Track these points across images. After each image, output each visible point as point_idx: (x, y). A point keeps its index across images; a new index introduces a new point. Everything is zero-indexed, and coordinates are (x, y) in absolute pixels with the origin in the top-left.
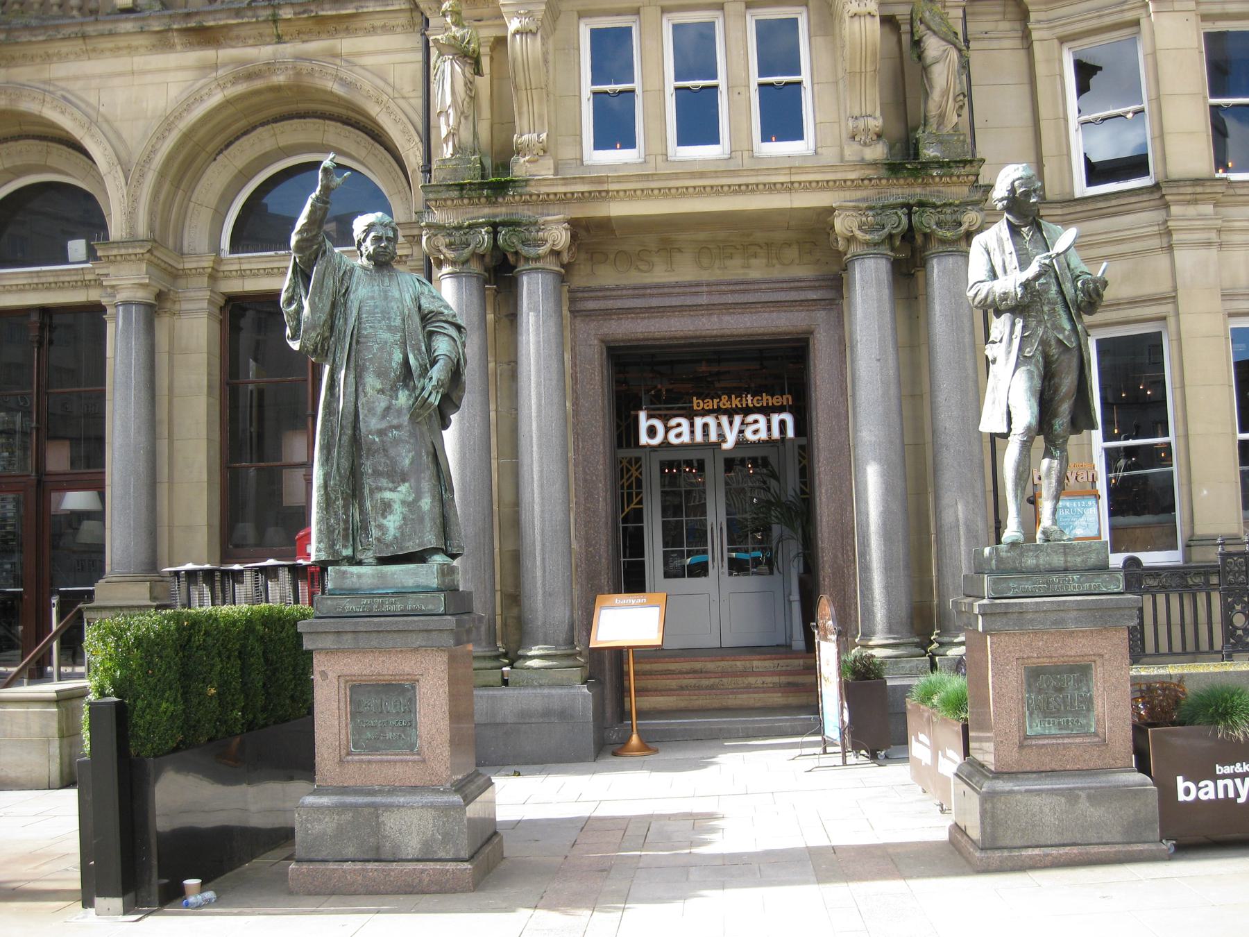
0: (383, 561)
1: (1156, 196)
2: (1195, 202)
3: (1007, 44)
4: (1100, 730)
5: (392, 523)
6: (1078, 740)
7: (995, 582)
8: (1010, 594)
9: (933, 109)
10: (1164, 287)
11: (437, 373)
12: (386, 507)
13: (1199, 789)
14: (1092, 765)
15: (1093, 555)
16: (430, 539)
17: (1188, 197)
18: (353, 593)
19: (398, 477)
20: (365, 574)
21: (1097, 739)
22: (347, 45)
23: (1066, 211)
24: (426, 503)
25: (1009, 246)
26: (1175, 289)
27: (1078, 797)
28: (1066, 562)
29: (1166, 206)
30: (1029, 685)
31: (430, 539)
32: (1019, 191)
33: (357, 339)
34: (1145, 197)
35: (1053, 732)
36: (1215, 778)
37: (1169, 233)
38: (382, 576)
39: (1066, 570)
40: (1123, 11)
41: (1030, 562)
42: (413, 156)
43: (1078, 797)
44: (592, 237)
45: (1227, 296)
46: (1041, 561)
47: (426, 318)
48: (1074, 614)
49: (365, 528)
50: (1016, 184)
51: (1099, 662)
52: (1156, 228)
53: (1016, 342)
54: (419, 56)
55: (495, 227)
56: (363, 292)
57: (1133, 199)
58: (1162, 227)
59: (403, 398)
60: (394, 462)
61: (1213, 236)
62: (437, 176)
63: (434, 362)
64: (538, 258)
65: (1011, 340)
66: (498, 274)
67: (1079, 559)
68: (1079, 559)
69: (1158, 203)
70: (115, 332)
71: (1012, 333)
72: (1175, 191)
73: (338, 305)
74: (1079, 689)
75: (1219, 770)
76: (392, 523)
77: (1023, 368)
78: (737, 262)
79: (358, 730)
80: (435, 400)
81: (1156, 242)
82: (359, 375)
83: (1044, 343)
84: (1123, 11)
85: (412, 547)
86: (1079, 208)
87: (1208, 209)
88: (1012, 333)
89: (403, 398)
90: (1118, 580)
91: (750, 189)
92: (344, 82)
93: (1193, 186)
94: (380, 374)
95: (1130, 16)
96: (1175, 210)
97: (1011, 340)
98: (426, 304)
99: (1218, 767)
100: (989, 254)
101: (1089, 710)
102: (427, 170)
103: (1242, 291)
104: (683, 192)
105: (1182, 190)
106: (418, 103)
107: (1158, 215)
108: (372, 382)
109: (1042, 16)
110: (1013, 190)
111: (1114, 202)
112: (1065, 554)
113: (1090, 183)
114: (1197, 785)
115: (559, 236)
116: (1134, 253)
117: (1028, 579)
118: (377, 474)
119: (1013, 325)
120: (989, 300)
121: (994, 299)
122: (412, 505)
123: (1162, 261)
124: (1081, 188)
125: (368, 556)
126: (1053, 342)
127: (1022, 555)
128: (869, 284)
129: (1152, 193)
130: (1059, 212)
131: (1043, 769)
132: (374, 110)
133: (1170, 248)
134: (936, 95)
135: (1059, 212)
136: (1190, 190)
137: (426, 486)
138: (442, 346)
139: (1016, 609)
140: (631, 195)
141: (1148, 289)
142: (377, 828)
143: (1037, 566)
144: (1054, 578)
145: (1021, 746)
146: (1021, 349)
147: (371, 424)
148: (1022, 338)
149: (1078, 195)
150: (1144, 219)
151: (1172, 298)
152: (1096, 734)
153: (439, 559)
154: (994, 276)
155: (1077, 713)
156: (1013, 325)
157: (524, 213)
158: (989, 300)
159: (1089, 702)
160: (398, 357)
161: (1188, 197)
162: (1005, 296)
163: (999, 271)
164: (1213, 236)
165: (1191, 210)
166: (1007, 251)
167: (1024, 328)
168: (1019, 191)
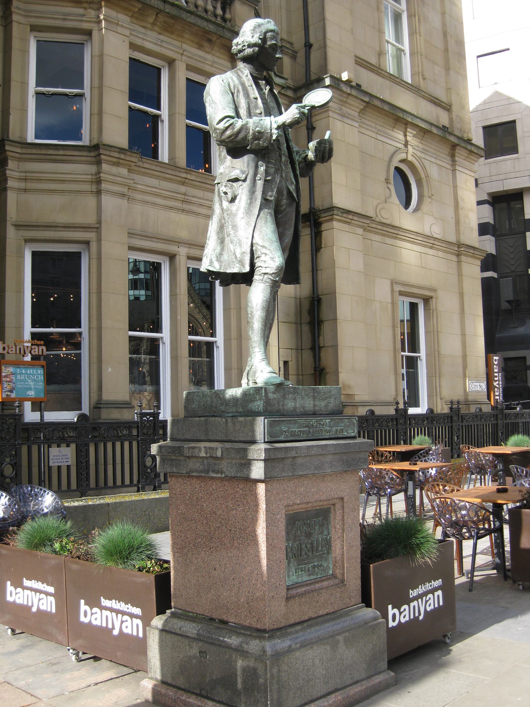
1: (93, 154)
2: (117, 164)
4: (338, 572)
6: (325, 584)
7: (271, 425)
8: (282, 438)
10: (91, 220)
13: (400, 613)
14: (336, 608)
15: (332, 400)
17: (115, 160)
21: (337, 581)
23: (24, 151)
25: (254, 93)
26: (99, 222)
27: (338, 641)
28: (315, 406)
29: (99, 163)
30: (288, 533)
32: (269, 43)
34: (85, 153)
35: (305, 578)
36: (408, 601)
37: (99, 182)
39: (314, 414)
40: (82, 21)
41: (290, 405)
43: (338, 641)
45: (131, 234)
46: (298, 405)
48: (329, 458)
50: (269, 35)
51: (338, 506)
52: (90, 177)
53: (260, 184)
57: (76, 153)
58: (94, 177)
65: (254, 181)
67: (323, 404)
68: (323, 404)
69: (93, 159)
71: (255, 175)
72: (107, 153)
74: (322, 533)
75: (413, 593)
77: (266, 210)
81: (87, 187)
83: (279, 192)
84: (82, 21)
86: (34, 151)
87: (124, 171)
88: (255, 175)
90: (354, 425)
93: (119, 153)
95: (86, 26)
96: (105, 167)
97: (254, 181)
99: (411, 592)
100: (233, 94)
101: (328, 553)
103: (139, 233)
105: (112, 154)
107: (93, 169)
110: (264, 40)
111: (61, 152)
112: (314, 398)
113: (37, 137)
114: (399, 610)
116: (71, 192)
117: (295, 422)
119: (257, 167)
120: (241, 136)
121: (245, 138)
123: (91, 201)
124: (31, 138)
126: (285, 192)
127: (284, 397)
129: (90, 151)
130: (19, 150)
131: (303, 618)
133: (99, 192)
135: (19, 150)
136: (117, 155)
139: (293, 454)
141: (79, 220)
143: (295, 408)
144: (313, 421)
145: (288, 599)
146: (264, 193)
148: (266, 181)
149: (29, 141)
150: (82, 170)
151: (97, 228)
152: (334, 576)
154: (238, 116)
155: (321, 557)
156: (257, 167)
158: (241, 136)
159: (328, 544)
161: (115, 160)
162: (259, 135)
163: (243, 112)
165: (114, 170)
166: (252, 96)
167: (267, 172)
168: (269, 43)
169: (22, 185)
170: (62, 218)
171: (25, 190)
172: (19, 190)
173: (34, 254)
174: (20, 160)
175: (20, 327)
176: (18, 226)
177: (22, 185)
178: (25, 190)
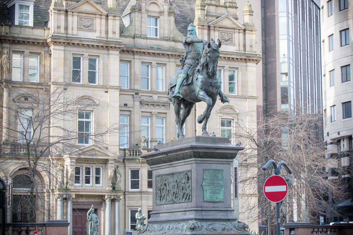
3: (122, 168)
9: (117, 183)
37: (142, 198)
44: (78, 196)
61: (147, 199)
78: (90, 199)
81: (140, 199)
87: (146, 195)
91: (96, 192)
104: (88, 192)
107: (141, 195)
109: (127, 165)
115: (74, 197)
123: (140, 201)
128: (108, 203)
133: (142, 200)
134: (118, 181)
140: (82, 192)
157: (70, 193)
164: (147, 199)
165: (145, 195)
169: (128, 199)
170: (135, 205)
171: (129, 200)
172: (128, 200)
173: (131, 211)
174: (128, 194)
175: (128, 224)
176: (128, 207)
177: (128, 199)
178: (129, 200)
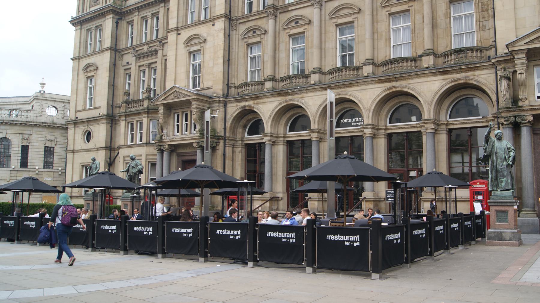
0: (501, 191)
5: (503, 184)
11: (511, 159)
12: (502, 182)
16: (510, 187)
18: (497, 196)
19: (504, 176)
20: (499, 193)
22: (477, 73)
24: (509, 181)
31: (510, 187)
33: (496, 153)
38: (502, 194)
42: (494, 98)
47: (508, 149)
49: (498, 185)
54: (495, 74)
55: (515, 117)
56: (497, 144)
59: (505, 163)
60: (503, 174)
62: (501, 105)
63: (510, 157)
64: (525, 123)
66: (516, 127)
70: (425, 139)
73: (493, 147)
76: (503, 184)
79: (498, 219)
80: (511, 163)
82: (497, 159)
85: (507, 188)
89: (505, 163)
92: (477, 81)
94: (501, 159)
98: (509, 146)
102: (498, 102)
106: (495, 85)
108: (499, 160)
118: (500, 176)
122: (507, 181)
125: (499, 190)
132: (484, 88)
137: (509, 178)
138: (512, 154)
142: (501, 236)
147: (499, 167)
153: (512, 190)
157: (522, 113)
160: (504, 156)
